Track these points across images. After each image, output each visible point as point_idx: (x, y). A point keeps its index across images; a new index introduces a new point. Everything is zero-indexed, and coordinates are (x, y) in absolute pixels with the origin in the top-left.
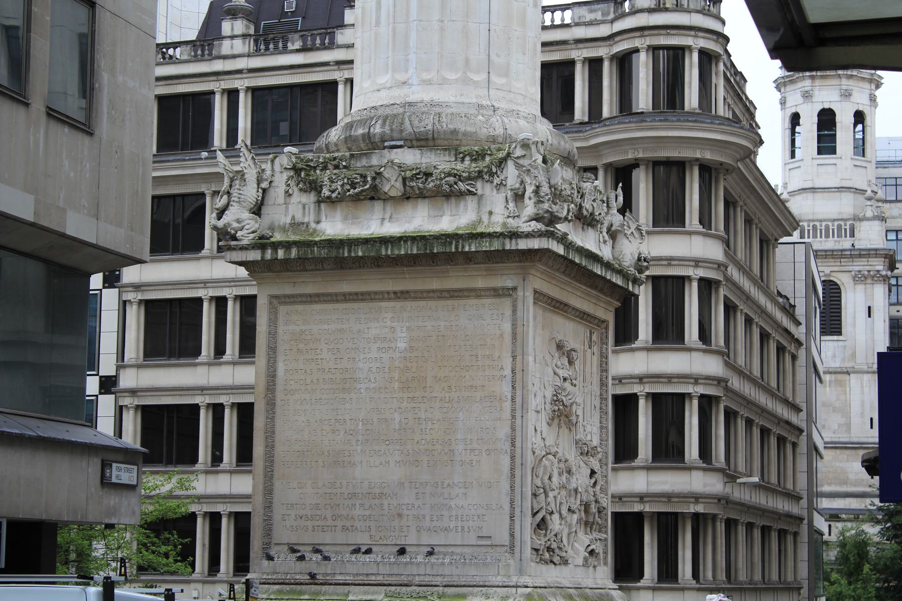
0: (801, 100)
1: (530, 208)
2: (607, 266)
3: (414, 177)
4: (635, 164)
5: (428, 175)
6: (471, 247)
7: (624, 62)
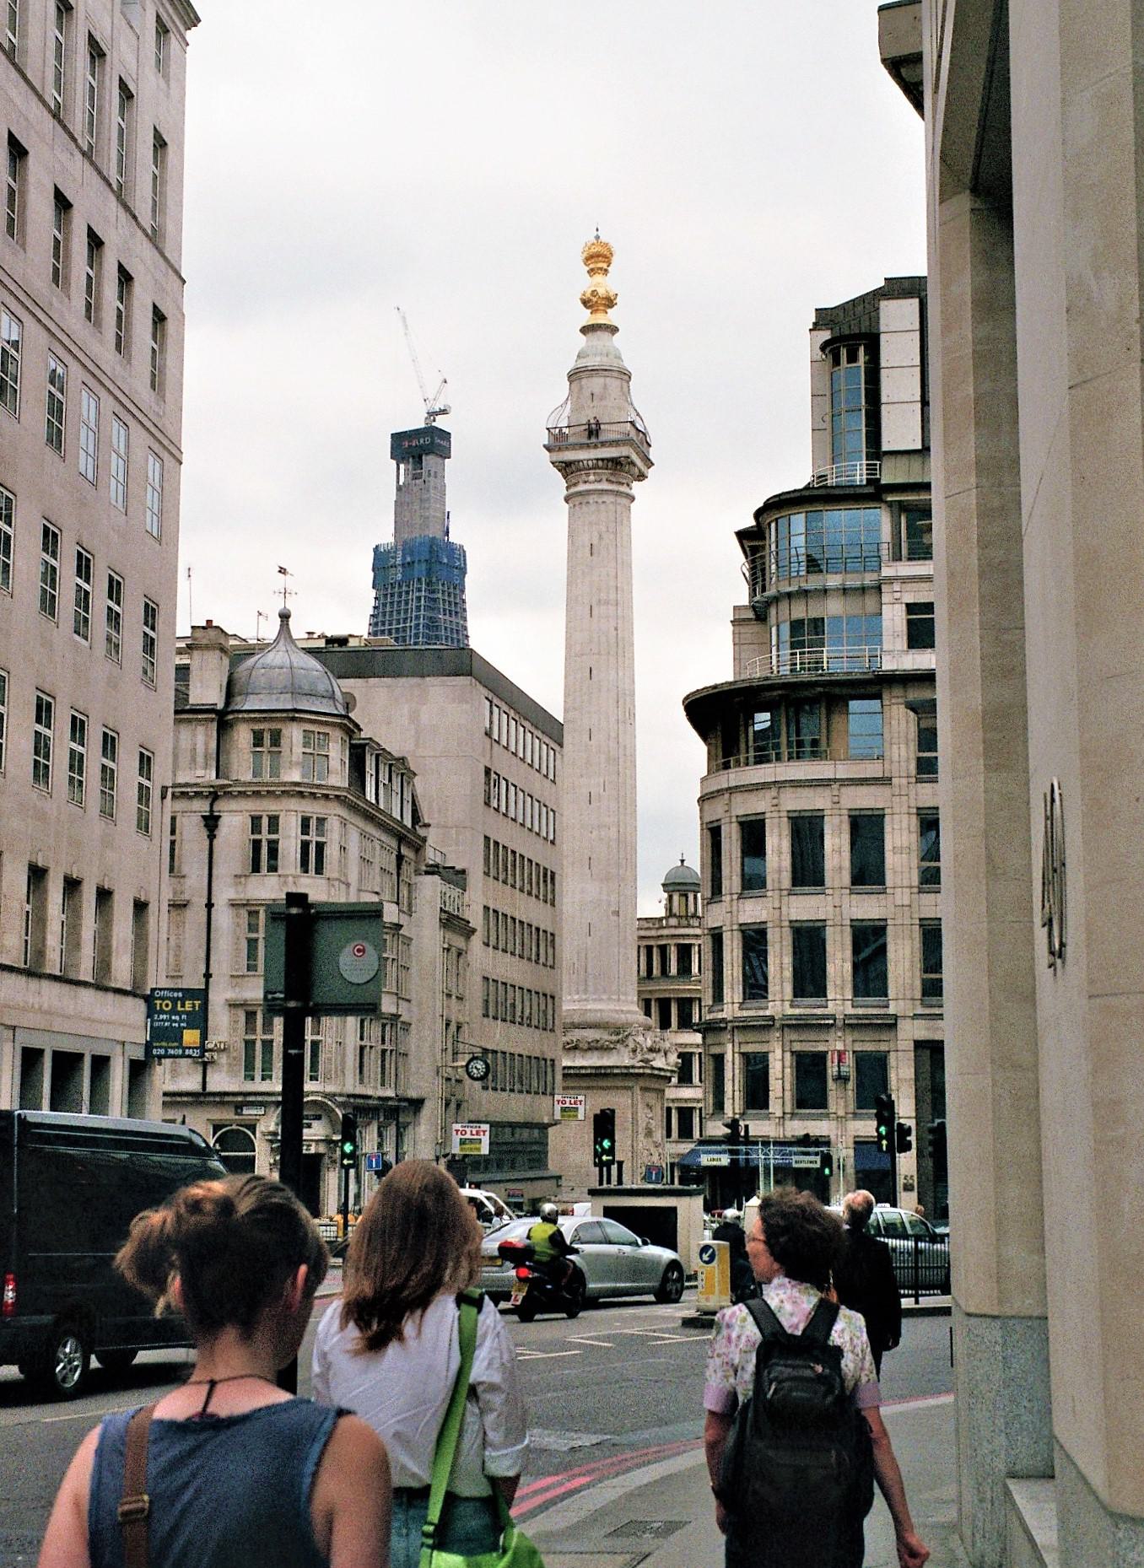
1: (639, 1057)
7: (663, 949)
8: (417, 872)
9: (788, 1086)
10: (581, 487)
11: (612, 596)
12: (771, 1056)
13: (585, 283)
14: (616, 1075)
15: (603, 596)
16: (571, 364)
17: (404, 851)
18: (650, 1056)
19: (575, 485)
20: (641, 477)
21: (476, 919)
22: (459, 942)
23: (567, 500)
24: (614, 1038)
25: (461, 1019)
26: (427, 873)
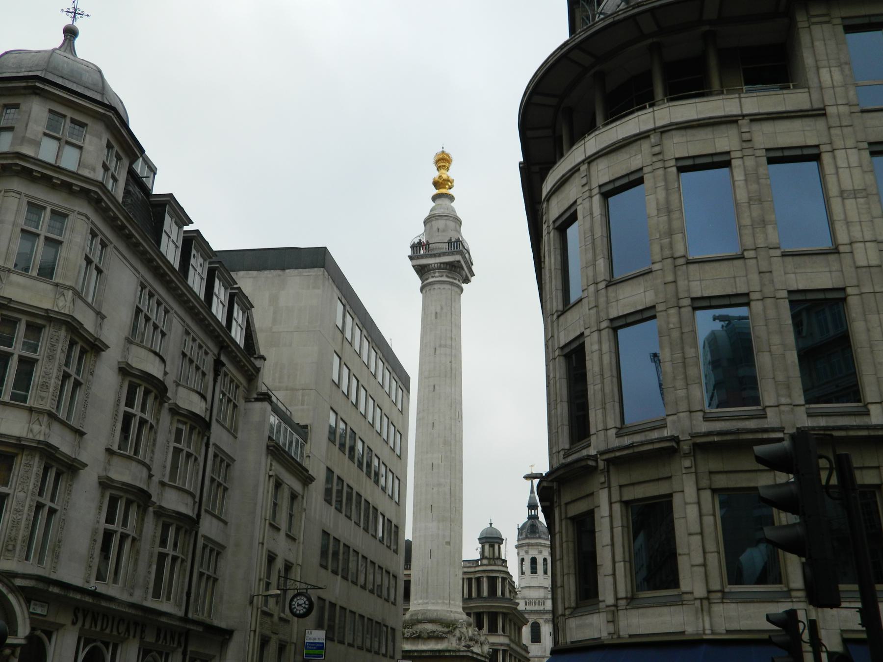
1: (463, 644)
2: (482, 656)
4: (483, 613)
6: (447, 654)
7: (478, 580)
8: (247, 400)
9: (711, 546)
10: (431, 280)
11: (449, 342)
12: (677, 500)
13: (435, 174)
14: (446, 657)
15: (443, 342)
16: (426, 214)
17: (223, 358)
18: (471, 643)
19: (427, 279)
21: (317, 470)
22: (291, 482)
24: (446, 630)
25: (292, 559)
26: (257, 400)
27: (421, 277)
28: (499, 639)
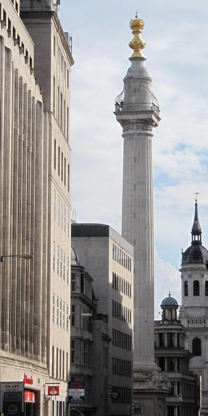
0: (188, 277)
1: (157, 385)
3: (136, 378)
5: (138, 378)
6: (147, 391)
13: (131, 37)
16: (125, 75)
19: (127, 130)
20: (156, 125)
23: (123, 136)
24: (145, 377)
27: (123, 125)
28: (176, 375)
